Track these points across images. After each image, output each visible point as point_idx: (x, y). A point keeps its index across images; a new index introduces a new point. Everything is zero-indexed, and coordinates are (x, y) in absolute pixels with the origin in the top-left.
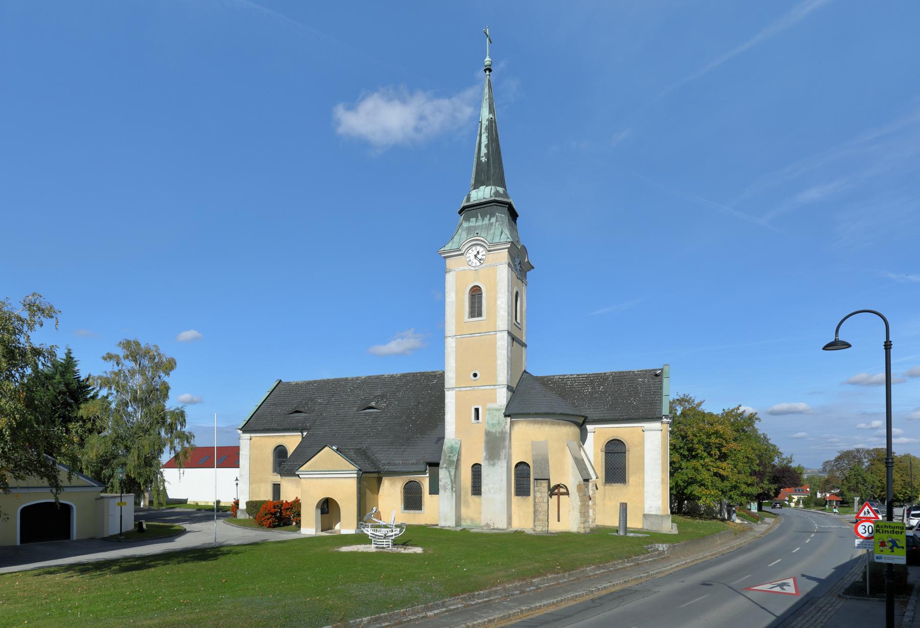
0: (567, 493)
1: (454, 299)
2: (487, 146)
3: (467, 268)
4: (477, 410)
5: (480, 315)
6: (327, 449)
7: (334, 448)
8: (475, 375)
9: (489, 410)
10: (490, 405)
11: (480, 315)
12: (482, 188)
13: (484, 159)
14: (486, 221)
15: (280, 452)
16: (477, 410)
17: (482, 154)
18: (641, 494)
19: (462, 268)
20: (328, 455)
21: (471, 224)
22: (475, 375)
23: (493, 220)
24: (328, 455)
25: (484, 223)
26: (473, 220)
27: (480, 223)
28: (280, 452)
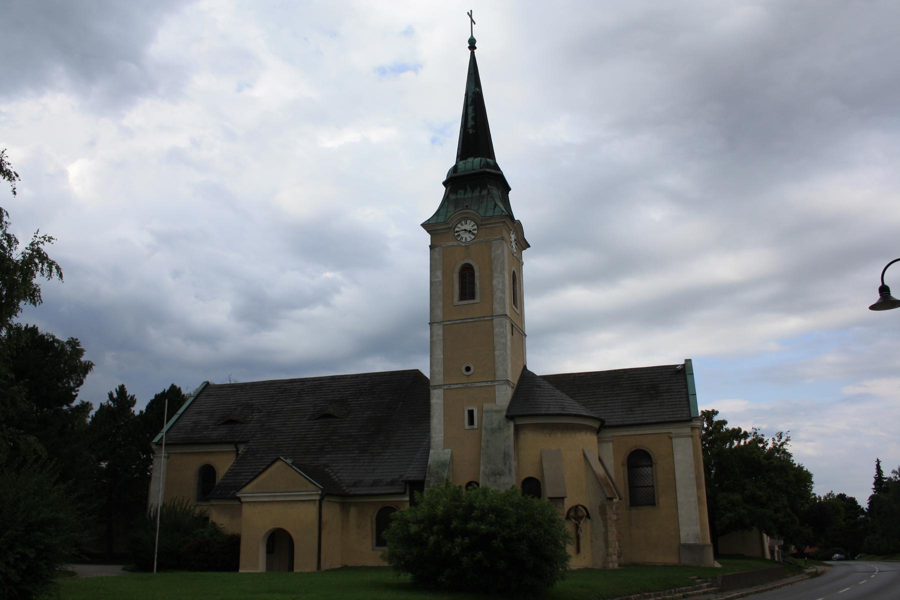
0: (588, 516)
1: (441, 279)
2: (473, 118)
3: (455, 243)
4: (471, 413)
5: (472, 296)
6: (278, 464)
7: (289, 461)
8: (468, 369)
9: (487, 412)
10: (487, 406)
11: (472, 296)
12: (470, 160)
13: (471, 131)
14: (476, 193)
15: (207, 473)
16: (471, 413)
17: (469, 126)
18: (675, 517)
19: (450, 244)
20: (280, 472)
21: (459, 196)
22: (468, 369)
23: (485, 192)
24: (280, 472)
25: (474, 195)
26: (462, 191)
27: (470, 195)
28: (207, 473)
